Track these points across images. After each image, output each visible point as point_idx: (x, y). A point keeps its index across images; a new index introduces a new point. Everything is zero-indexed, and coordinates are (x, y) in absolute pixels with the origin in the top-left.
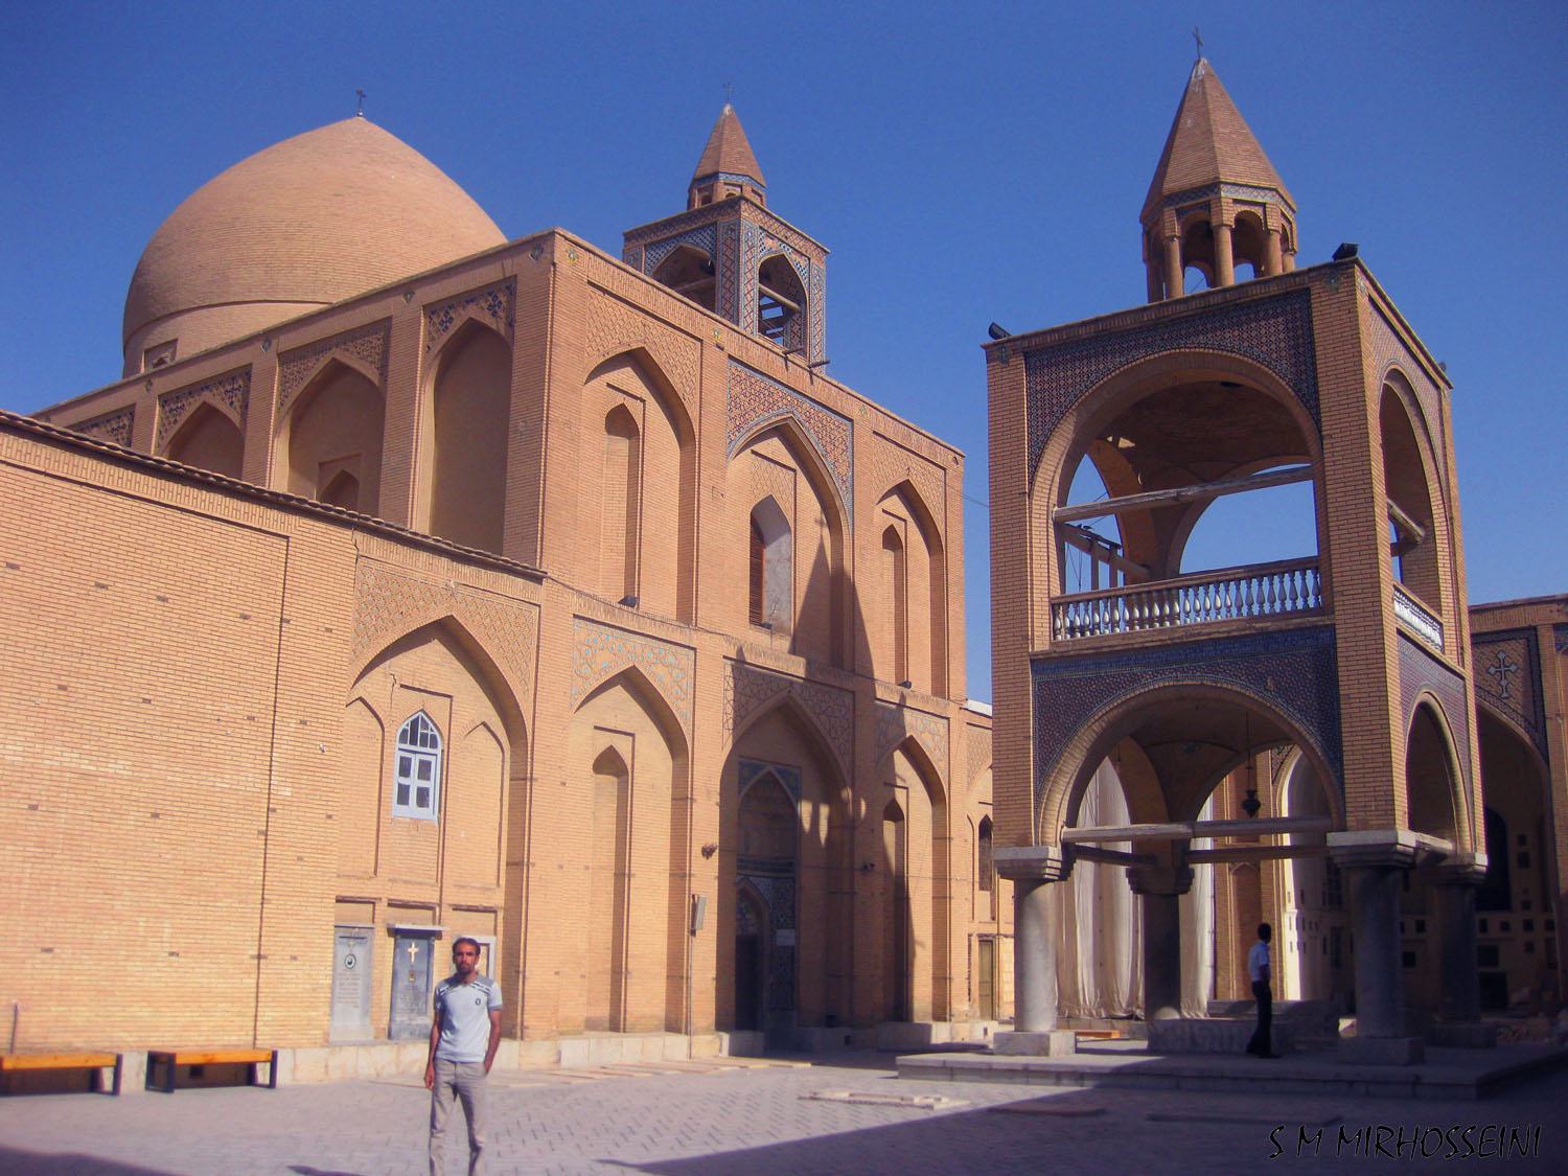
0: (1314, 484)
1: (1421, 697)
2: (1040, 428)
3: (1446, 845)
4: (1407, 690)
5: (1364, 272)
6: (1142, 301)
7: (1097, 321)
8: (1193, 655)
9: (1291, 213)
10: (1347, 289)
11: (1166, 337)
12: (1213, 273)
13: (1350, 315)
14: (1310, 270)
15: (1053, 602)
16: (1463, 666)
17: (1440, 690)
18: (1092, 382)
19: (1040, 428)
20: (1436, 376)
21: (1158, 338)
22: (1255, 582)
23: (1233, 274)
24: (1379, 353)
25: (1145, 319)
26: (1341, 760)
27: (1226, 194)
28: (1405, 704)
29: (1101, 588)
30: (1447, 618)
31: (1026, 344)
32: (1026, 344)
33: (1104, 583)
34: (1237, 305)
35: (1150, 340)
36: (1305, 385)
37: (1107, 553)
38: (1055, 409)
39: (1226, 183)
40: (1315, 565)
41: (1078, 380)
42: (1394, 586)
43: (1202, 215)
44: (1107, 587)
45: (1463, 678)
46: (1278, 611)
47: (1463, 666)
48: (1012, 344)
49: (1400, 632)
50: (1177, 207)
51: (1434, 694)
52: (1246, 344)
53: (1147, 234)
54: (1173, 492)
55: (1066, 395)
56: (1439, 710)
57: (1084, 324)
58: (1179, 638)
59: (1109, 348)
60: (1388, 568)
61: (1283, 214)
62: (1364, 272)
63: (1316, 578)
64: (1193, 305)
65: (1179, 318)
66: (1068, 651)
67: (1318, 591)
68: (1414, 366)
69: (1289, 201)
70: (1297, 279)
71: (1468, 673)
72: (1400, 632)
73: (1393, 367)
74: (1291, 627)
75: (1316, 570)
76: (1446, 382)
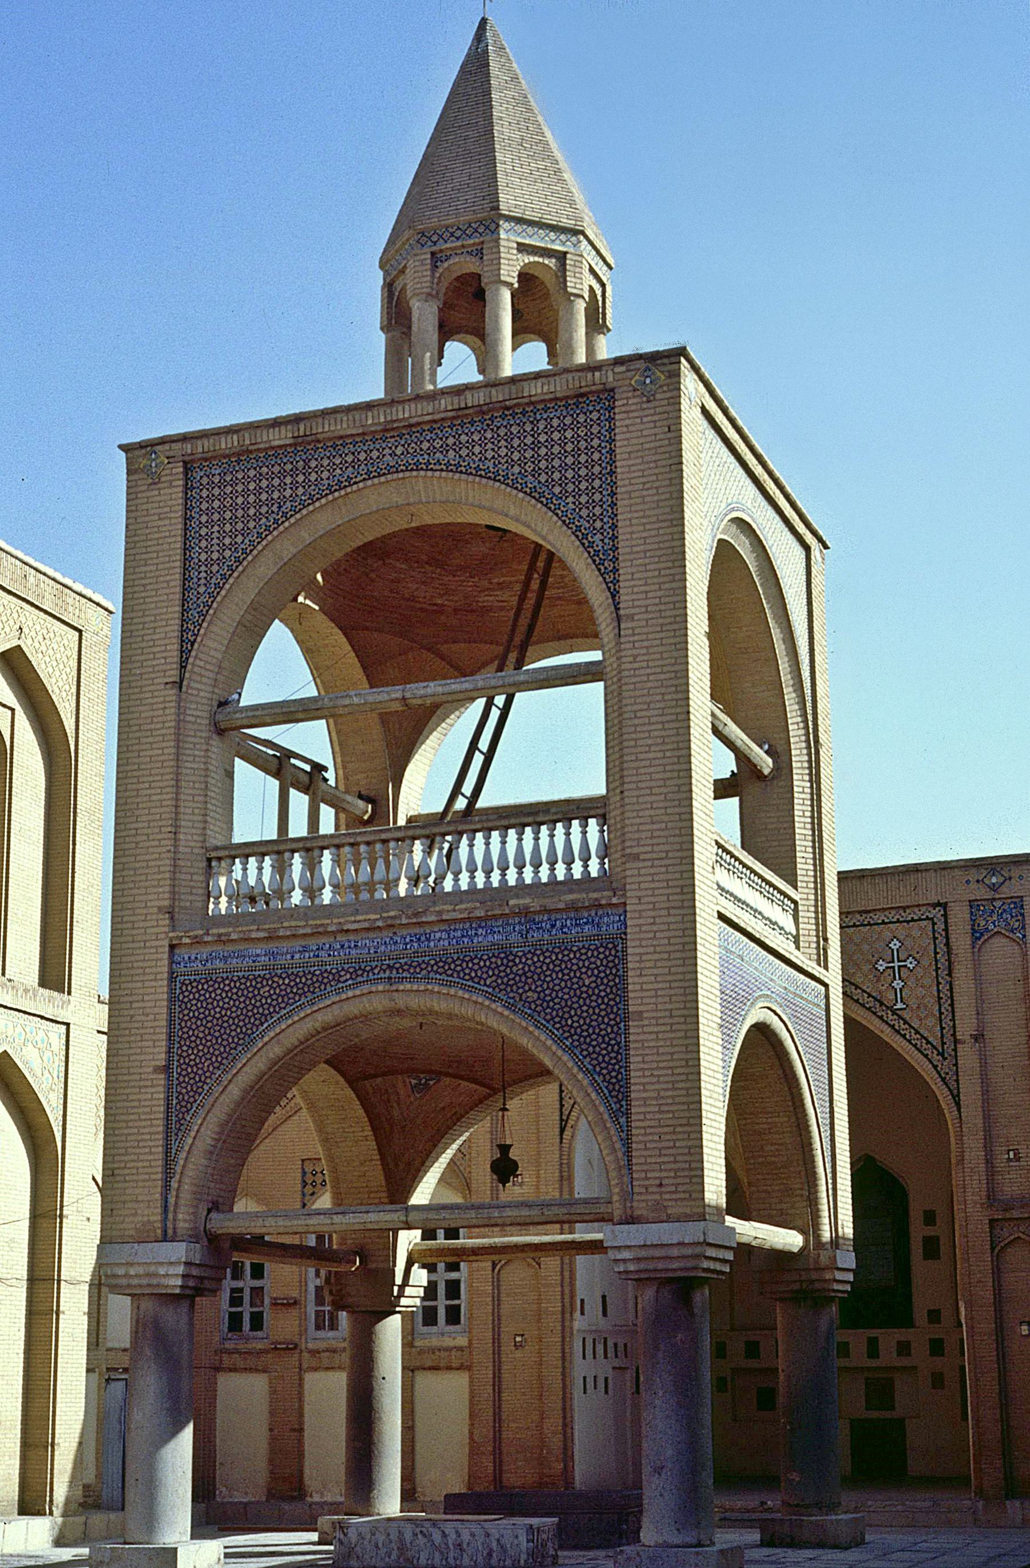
0: (606, 688)
1: (756, 1015)
2: (203, 581)
3: (791, 1240)
4: (733, 1002)
5: (696, 369)
6: (377, 391)
7: (297, 419)
8: (416, 945)
9: (605, 268)
10: (668, 395)
11: (398, 452)
12: (487, 358)
13: (669, 435)
16: (826, 968)
17: (788, 1004)
18: (285, 514)
19: (203, 581)
20: (807, 538)
21: (387, 451)
22: (512, 833)
23: (522, 359)
24: (713, 495)
25: (370, 422)
26: (628, 1114)
27: (508, 236)
28: (726, 1027)
29: (322, 832)
30: (803, 894)
33: (298, 828)
34: (508, 408)
35: (375, 454)
37: (305, 779)
39: (509, 218)
40: (600, 811)
41: (264, 509)
42: (717, 843)
43: (471, 265)
44: (332, 831)
45: (826, 986)
46: (544, 880)
47: (826, 968)
49: (721, 917)
50: (434, 249)
51: (779, 1011)
52: (516, 469)
53: (389, 287)
56: (784, 1035)
57: (276, 423)
59: (313, 464)
60: (716, 821)
61: (592, 271)
62: (696, 369)
63: (602, 831)
64: (444, 403)
65: (419, 424)
67: (605, 850)
68: (771, 512)
69: (603, 251)
71: (834, 977)
72: (721, 917)
73: (734, 515)
74: (562, 906)
75: (603, 819)
76: (820, 540)
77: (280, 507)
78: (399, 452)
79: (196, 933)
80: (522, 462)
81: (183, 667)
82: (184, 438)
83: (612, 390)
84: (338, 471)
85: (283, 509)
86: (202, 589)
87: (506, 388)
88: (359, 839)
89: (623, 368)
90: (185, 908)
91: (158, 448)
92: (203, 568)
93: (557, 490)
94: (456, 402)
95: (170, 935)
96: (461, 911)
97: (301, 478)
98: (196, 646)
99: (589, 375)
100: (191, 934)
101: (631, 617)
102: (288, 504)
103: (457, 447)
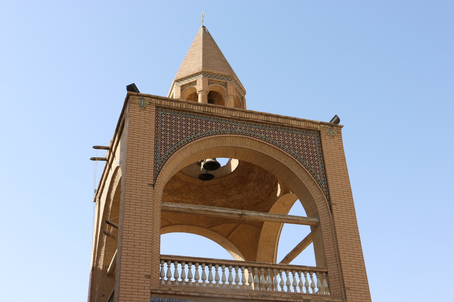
2: (163, 151)
14: (321, 123)
15: (162, 258)
19: (163, 151)
31: (158, 102)
32: (158, 102)
36: (318, 176)
38: (173, 143)
40: (326, 270)
48: (149, 99)
54: (240, 212)
55: (181, 138)
58: (256, 296)
59: (209, 123)
66: (180, 292)
70: (314, 125)
77: (196, 133)
78: (243, 128)
79: (164, 289)
80: (289, 144)
81: (155, 180)
82: (157, 98)
83: (319, 132)
84: (219, 128)
85: (197, 134)
86: (163, 153)
87: (284, 120)
88: (230, 263)
89: (323, 126)
90: (154, 278)
91: (145, 98)
92: (163, 146)
93: (302, 157)
94: (265, 118)
95: (152, 288)
96: (284, 298)
97: (204, 126)
98: (160, 173)
99: (312, 125)
100: (162, 289)
101: (335, 204)
102: (199, 133)
103: (265, 133)
